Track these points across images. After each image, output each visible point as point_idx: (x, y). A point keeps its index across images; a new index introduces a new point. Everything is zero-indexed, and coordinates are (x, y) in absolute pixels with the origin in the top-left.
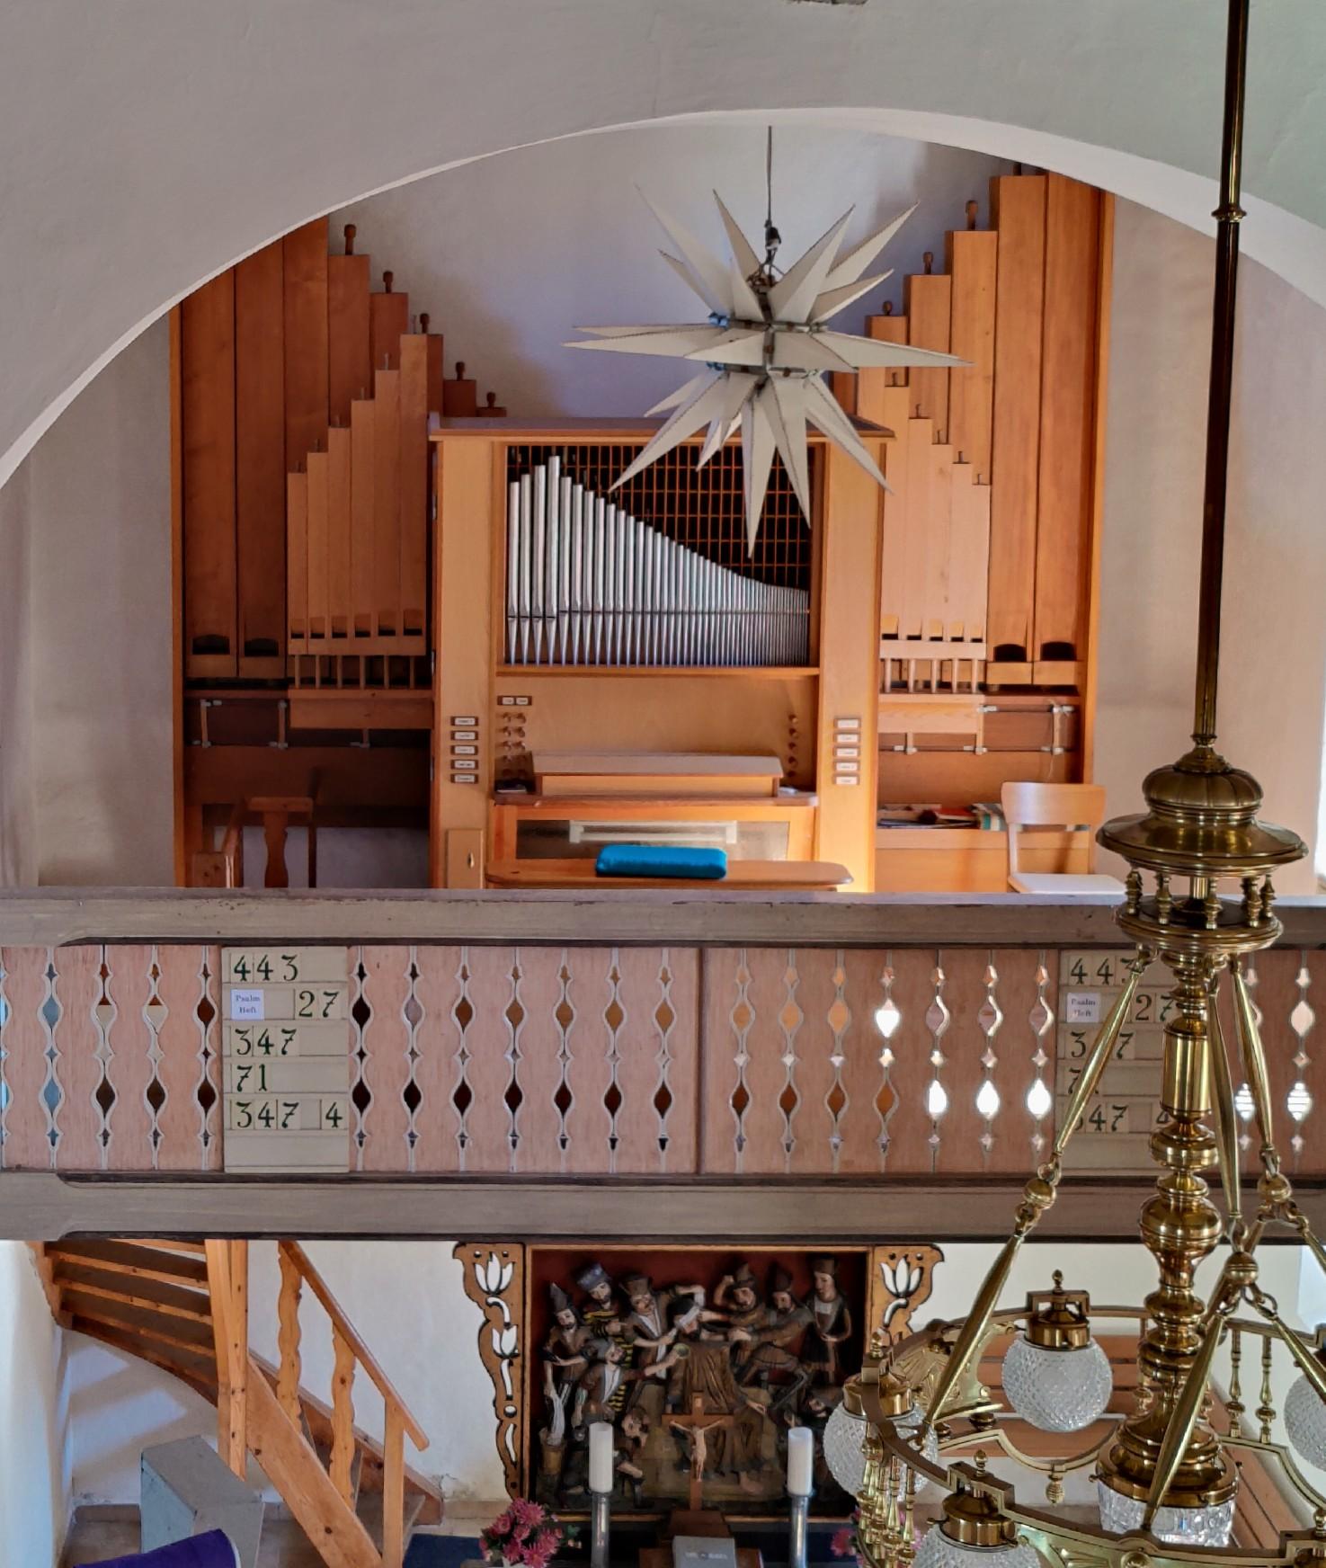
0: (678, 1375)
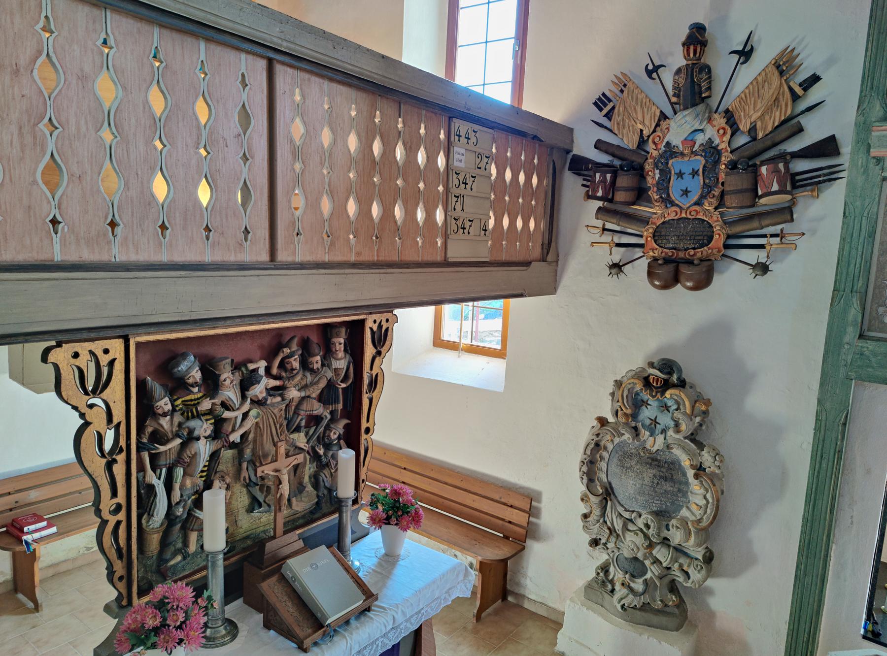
0: (251, 436)
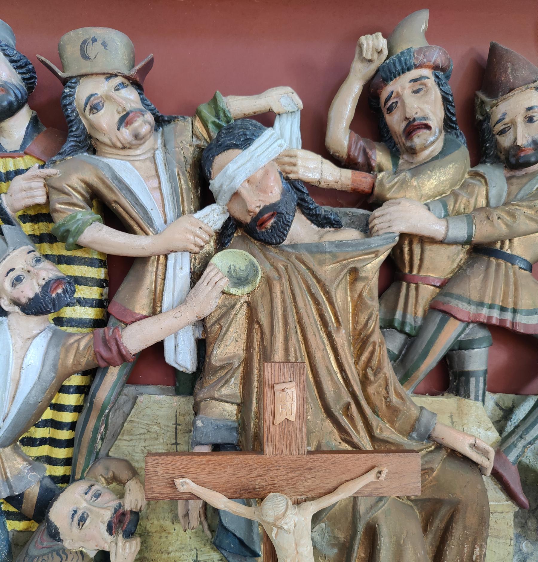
0: (229, 347)
